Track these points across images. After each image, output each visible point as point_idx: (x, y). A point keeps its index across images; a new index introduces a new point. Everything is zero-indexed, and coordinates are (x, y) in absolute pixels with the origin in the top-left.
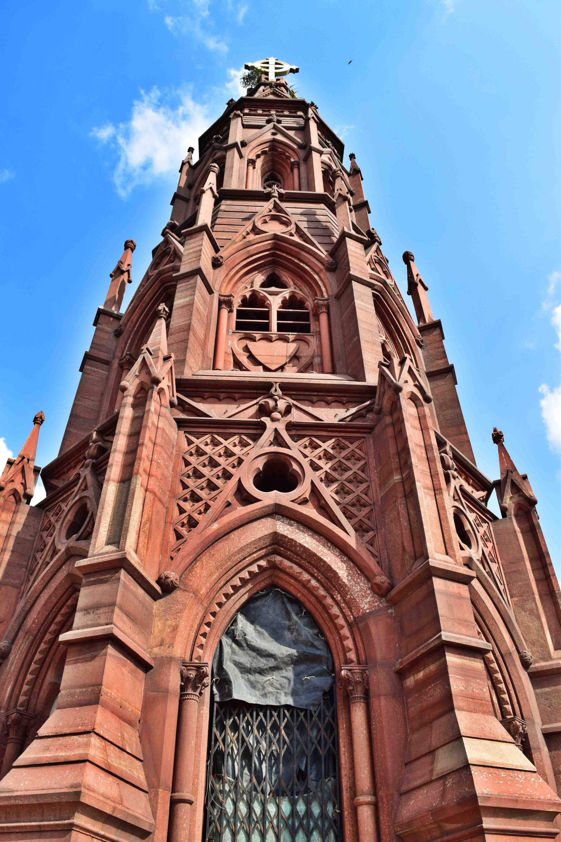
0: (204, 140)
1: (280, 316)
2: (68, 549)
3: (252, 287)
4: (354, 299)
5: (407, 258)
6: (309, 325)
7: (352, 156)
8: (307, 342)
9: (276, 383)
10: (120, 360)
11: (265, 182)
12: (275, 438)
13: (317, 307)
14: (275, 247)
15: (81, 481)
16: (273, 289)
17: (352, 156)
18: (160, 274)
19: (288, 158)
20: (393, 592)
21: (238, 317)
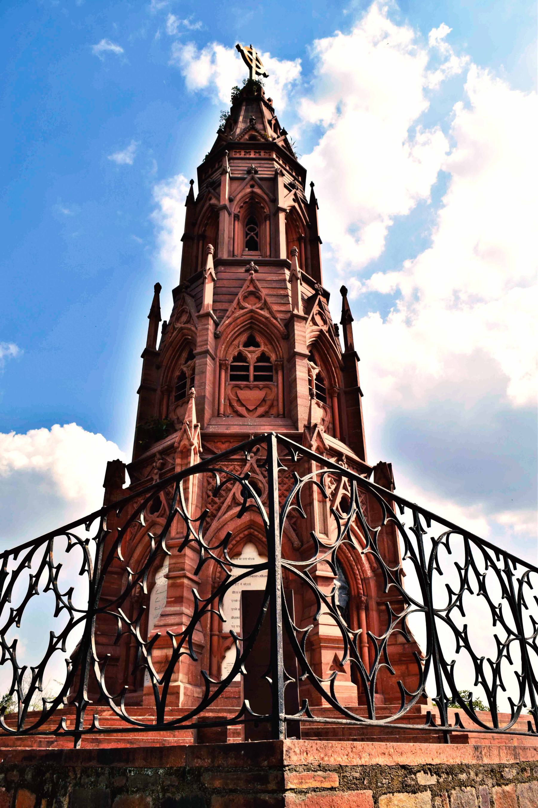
0: (201, 170)
1: (256, 369)
2: (152, 521)
3: (239, 347)
4: (296, 371)
5: (344, 291)
6: (271, 376)
7: (312, 185)
8: (270, 389)
9: (252, 434)
10: (162, 388)
11: (246, 226)
12: (251, 468)
13: (276, 365)
14: (252, 318)
15: (154, 482)
16: (252, 348)
17: (312, 185)
18: (182, 329)
19: (263, 208)
20: (302, 549)
21: (231, 371)
